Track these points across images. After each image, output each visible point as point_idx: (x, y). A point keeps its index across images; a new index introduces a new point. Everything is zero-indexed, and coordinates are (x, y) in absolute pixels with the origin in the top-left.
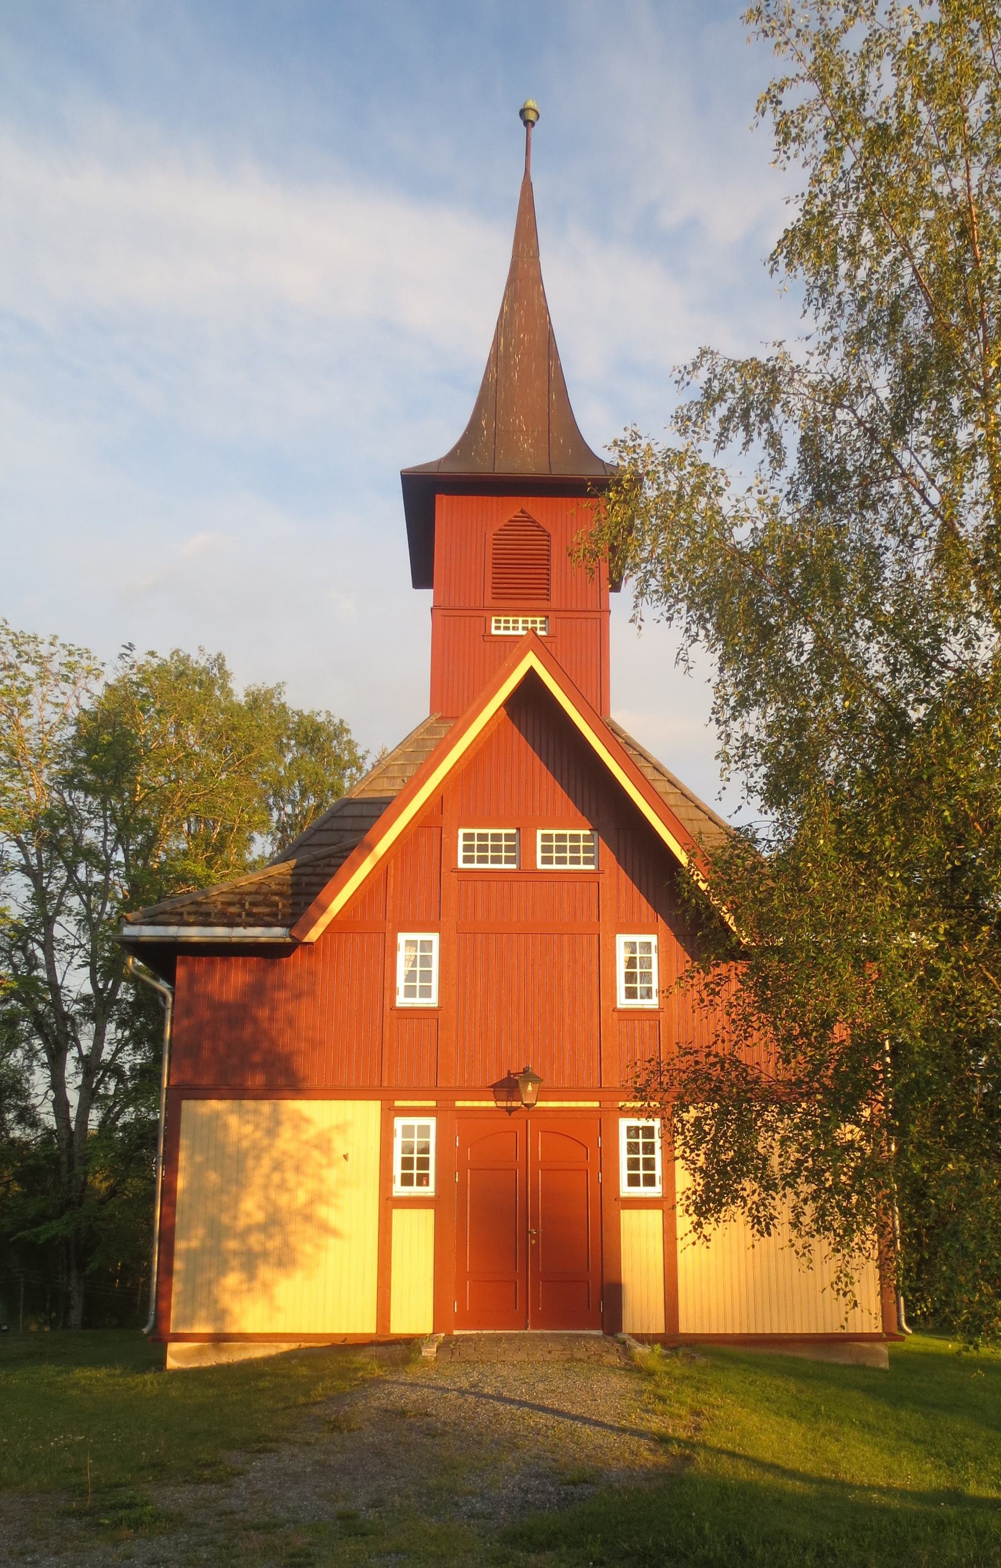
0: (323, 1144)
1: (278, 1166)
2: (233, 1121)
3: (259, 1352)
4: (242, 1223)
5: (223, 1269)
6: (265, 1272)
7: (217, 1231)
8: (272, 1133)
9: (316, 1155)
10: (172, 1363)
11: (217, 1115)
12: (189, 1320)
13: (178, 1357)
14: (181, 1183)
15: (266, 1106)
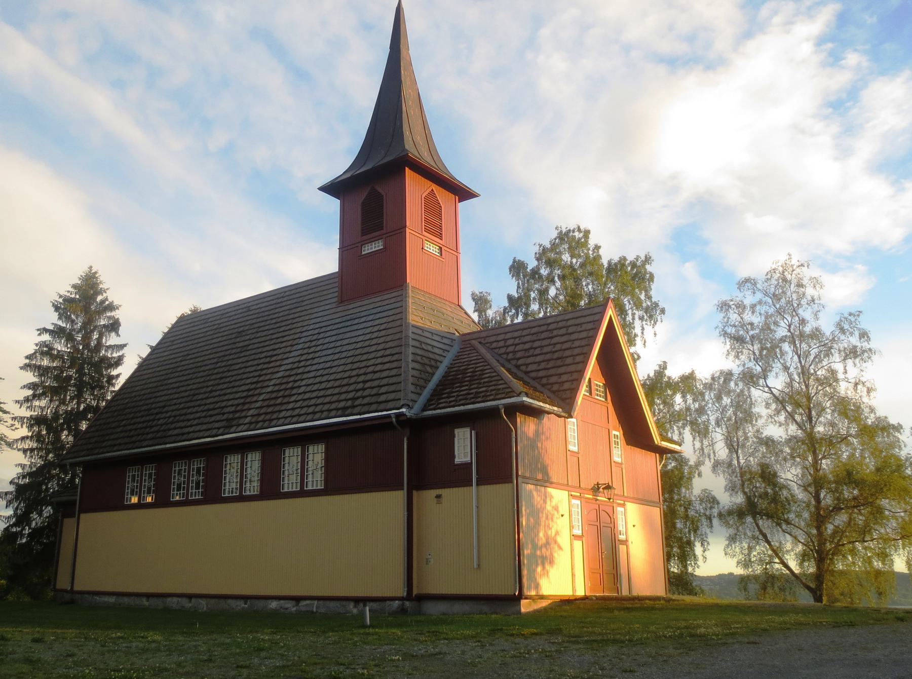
0: (556, 509)
1: (547, 518)
2: (535, 493)
3: (544, 604)
4: (540, 543)
5: (537, 566)
6: (547, 567)
7: (535, 546)
8: (545, 502)
9: (556, 513)
10: (523, 610)
11: (531, 491)
12: (529, 589)
13: (525, 607)
14: (524, 522)
15: (543, 489)
